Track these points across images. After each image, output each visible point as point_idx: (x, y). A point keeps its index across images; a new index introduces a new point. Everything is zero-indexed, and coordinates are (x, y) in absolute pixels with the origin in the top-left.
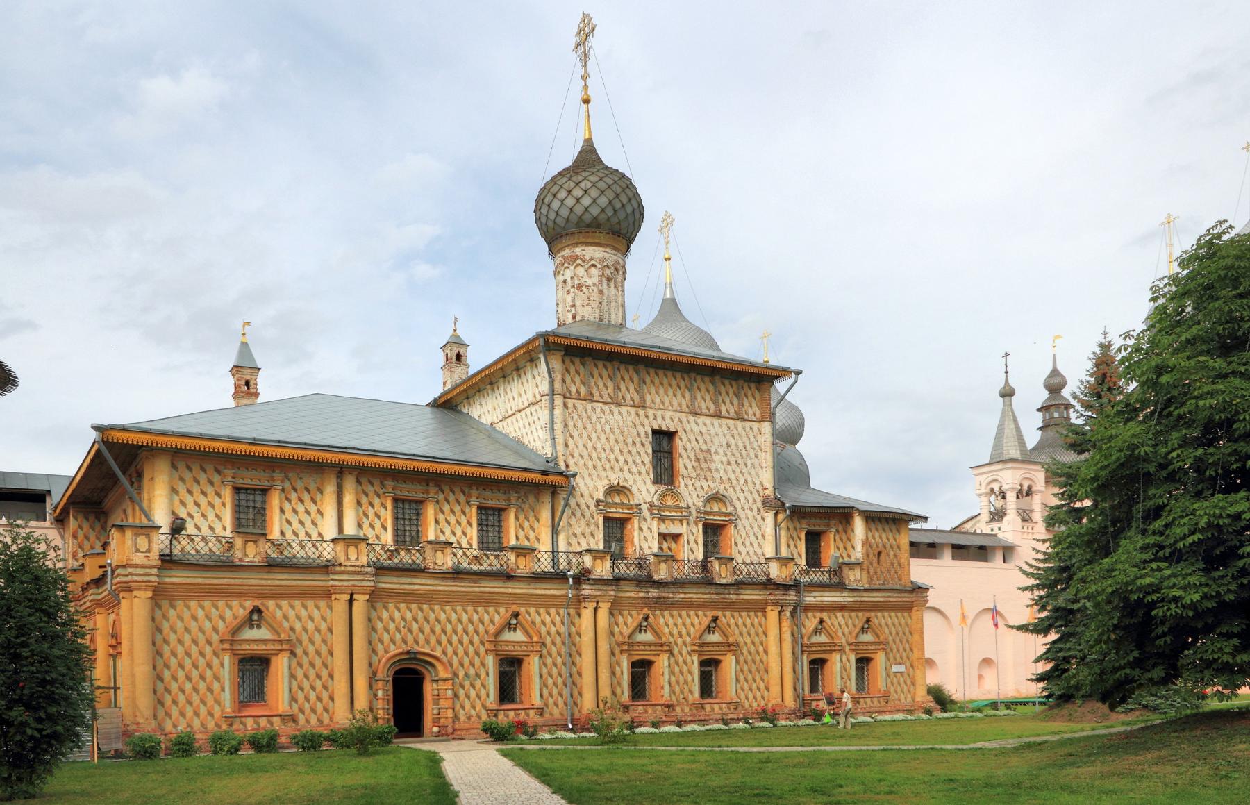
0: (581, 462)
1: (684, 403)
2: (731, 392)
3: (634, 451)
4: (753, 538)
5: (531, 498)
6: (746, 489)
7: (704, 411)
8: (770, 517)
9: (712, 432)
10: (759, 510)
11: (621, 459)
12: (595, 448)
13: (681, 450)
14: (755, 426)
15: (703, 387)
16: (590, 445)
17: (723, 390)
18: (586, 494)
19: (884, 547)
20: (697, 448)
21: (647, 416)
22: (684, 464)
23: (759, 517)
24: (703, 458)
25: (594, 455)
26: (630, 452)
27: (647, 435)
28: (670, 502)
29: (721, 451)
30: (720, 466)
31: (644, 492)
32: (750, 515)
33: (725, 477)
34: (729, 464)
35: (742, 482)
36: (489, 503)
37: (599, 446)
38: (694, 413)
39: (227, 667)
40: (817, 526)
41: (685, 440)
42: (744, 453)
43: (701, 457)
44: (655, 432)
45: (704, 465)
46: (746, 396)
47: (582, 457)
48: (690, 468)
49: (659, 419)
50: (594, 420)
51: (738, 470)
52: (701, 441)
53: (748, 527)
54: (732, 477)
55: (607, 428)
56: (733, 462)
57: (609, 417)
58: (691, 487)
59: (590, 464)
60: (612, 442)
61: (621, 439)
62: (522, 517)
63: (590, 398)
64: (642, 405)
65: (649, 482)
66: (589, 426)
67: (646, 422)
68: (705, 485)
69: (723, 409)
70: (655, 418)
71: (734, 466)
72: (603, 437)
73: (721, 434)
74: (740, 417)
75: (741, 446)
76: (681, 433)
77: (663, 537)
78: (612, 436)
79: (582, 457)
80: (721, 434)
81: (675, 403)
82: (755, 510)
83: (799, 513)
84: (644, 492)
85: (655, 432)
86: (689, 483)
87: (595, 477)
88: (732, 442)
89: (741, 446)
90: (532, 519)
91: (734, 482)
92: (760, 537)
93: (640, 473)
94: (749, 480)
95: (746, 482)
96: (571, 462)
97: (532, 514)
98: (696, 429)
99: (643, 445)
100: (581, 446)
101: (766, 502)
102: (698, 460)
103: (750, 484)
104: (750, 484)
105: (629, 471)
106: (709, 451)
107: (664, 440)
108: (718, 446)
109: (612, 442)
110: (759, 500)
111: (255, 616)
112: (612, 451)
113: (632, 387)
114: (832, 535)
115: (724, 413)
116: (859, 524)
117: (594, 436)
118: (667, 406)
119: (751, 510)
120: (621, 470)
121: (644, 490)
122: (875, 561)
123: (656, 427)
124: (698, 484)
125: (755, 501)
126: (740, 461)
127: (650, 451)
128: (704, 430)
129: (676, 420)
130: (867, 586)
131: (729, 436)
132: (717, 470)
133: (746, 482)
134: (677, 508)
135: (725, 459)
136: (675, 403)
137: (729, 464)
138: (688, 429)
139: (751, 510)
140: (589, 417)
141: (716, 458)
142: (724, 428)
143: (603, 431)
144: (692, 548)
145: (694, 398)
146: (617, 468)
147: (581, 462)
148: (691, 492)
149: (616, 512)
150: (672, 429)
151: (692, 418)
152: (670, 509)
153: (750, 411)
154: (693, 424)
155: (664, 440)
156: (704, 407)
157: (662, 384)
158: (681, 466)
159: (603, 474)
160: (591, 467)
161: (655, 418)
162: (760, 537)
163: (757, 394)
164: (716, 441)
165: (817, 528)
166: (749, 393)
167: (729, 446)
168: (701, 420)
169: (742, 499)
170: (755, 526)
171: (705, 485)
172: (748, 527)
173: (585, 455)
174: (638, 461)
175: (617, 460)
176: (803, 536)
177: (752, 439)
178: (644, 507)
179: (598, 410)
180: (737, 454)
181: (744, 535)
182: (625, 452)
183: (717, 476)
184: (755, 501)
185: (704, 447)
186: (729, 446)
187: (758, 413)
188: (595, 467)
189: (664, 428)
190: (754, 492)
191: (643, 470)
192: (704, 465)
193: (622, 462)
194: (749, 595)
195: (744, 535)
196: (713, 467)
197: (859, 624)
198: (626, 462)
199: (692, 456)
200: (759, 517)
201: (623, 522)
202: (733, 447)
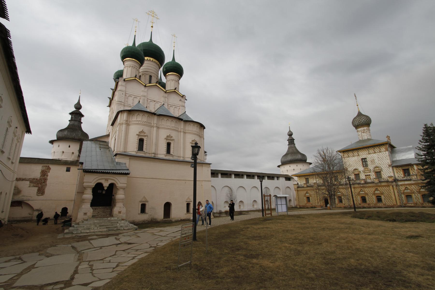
8: (391, 168)
22: (369, 163)
24: (373, 161)
28: (366, 170)
38: (369, 154)
39: (305, 198)
63: (349, 157)
64: (359, 155)
74: (380, 152)
77: (366, 175)
83: (397, 167)
85: (362, 159)
101: (389, 166)
107: (364, 161)
111: (307, 193)
114: (410, 169)
116: (415, 167)
118: (363, 154)
121: (361, 168)
144: (373, 176)
148: (371, 167)
155: (364, 161)
194: (383, 184)
201: (359, 174)
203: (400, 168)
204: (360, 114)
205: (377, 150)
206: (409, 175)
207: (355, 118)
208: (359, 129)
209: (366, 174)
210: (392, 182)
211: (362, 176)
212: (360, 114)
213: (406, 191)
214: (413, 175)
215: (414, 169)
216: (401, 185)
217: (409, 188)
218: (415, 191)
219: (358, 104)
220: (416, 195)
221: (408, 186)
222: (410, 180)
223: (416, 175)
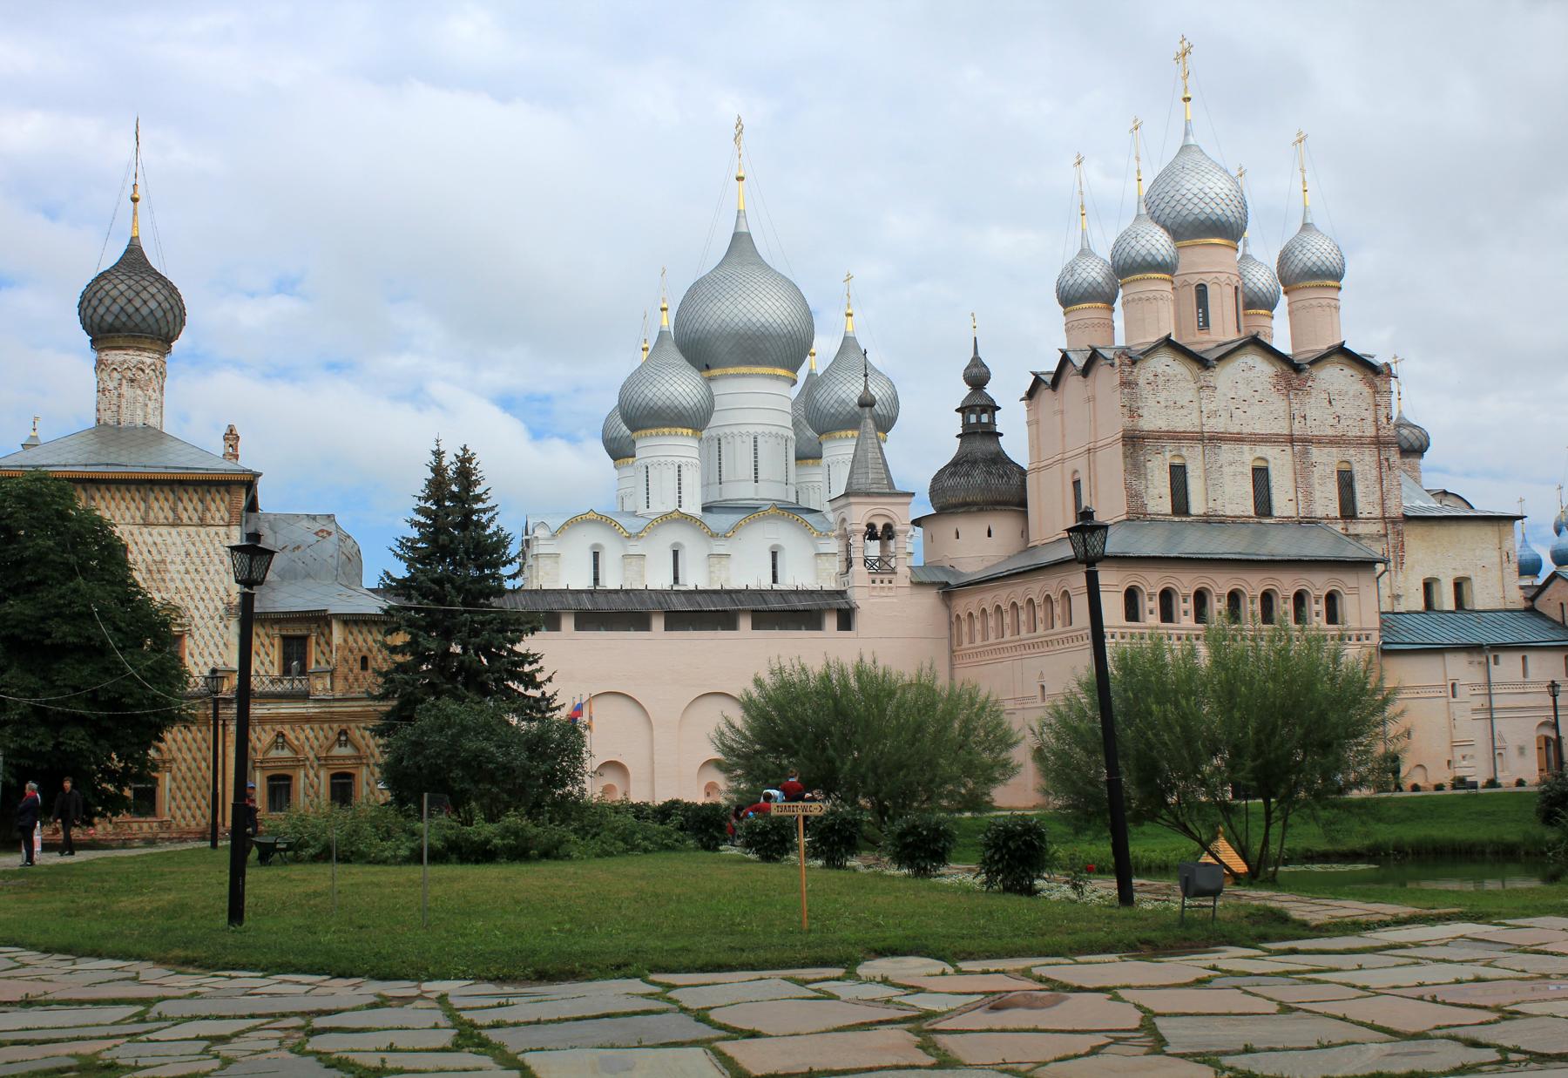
1: (138, 515)
2: (195, 498)
4: (212, 648)
6: (206, 597)
7: (162, 521)
9: (169, 541)
14: (222, 530)
15: (161, 497)
17: (185, 497)
19: (370, 650)
20: (149, 558)
29: (178, 560)
30: (175, 576)
32: (211, 624)
33: (181, 586)
34: (187, 572)
38: (146, 524)
40: (298, 631)
41: (135, 551)
42: (206, 560)
43: (154, 568)
45: (156, 576)
51: (198, 577)
52: (154, 552)
53: (207, 637)
54: (191, 586)
56: (192, 569)
69: (185, 516)
71: (194, 575)
73: (178, 542)
74: (202, 523)
75: (203, 552)
80: (178, 542)
81: (128, 516)
88: (193, 550)
89: (203, 552)
91: (193, 591)
94: (212, 588)
95: (207, 589)
98: (150, 540)
101: (228, 609)
102: (150, 571)
106: (163, 561)
108: (175, 557)
110: (221, 607)
115: (186, 520)
119: (212, 618)
122: (357, 667)
126: (201, 569)
128: (159, 540)
130: (338, 695)
131: (189, 545)
132: (172, 580)
133: (207, 589)
135: (182, 569)
136: (128, 516)
138: (140, 540)
141: (171, 568)
142: (184, 536)
145: (148, 508)
151: (145, 530)
153: (218, 515)
154: (146, 536)
156: (161, 515)
162: (221, 645)
163: (227, 498)
164: (173, 550)
165: (298, 633)
167: (187, 554)
168: (155, 531)
169: (202, 608)
170: (216, 635)
172: (207, 637)
176: (277, 642)
180: (197, 561)
181: (202, 645)
183: (172, 586)
185: (158, 558)
186: (187, 554)
187: (226, 517)
190: (216, 599)
192: (156, 576)
195: (202, 645)
196: (167, 577)
197: (332, 736)
200: (221, 626)
202: (193, 554)
203: (276, 631)
204: (134, 260)
205: (189, 506)
206: (303, 671)
207: (102, 276)
208: (115, 356)
212: (134, 260)
213: (273, 754)
214: (319, 674)
215: (329, 644)
216: (263, 721)
217: (291, 736)
218: (311, 755)
219: (140, 193)
220: (311, 773)
221: (287, 729)
222: (304, 696)
223: (332, 673)
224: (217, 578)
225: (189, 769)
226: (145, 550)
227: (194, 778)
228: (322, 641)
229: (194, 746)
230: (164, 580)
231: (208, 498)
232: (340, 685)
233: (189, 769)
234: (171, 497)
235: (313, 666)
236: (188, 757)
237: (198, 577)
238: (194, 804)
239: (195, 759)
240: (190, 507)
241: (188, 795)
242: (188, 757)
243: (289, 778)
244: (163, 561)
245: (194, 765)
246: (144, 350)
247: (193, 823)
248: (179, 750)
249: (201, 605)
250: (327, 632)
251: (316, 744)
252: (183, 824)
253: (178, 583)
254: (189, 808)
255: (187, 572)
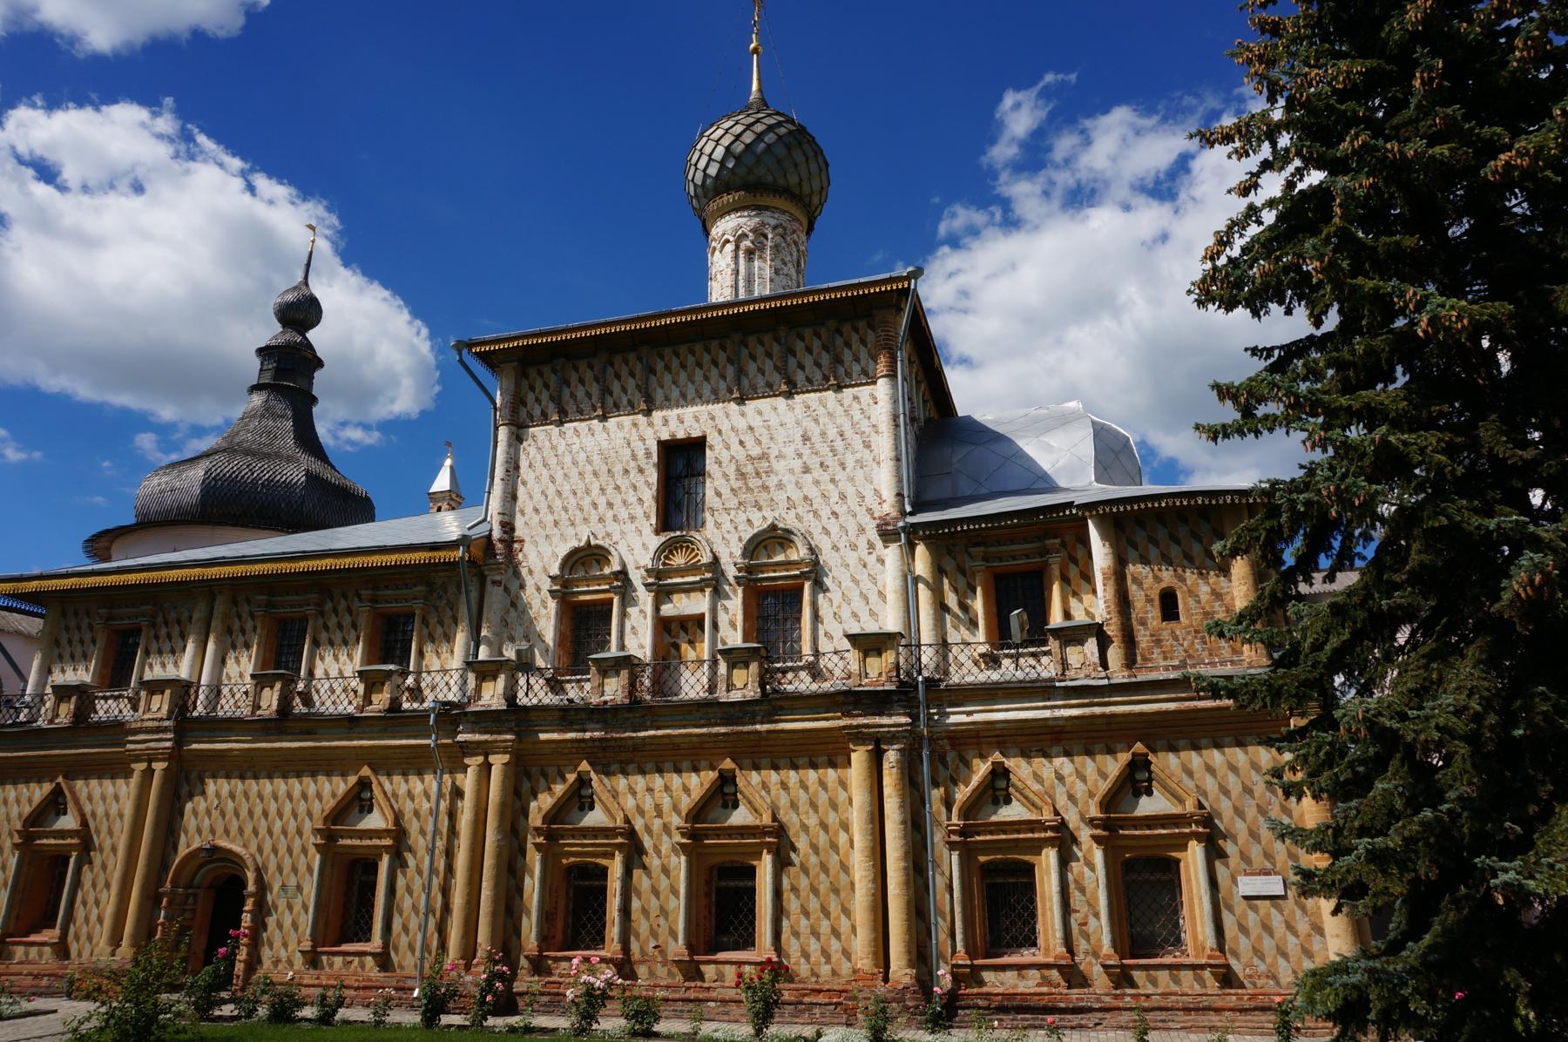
0: (536, 519)
3: (624, 483)
4: (858, 604)
5: (452, 589)
8: (892, 554)
9: (774, 422)
10: (871, 546)
11: (602, 501)
12: (559, 493)
13: (710, 465)
16: (551, 491)
18: (537, 569)
20: (740, 454)
21: (651, 424)
23: (871, 560)
25: (558, 504)
26: (617, 488)
27: (648, 455)
29: (789, 451)
31: (637, 546)
32: (852, 557)
33: (796, 496)
35: (835, 498)
36: (393, 607)
37: (566, 489)
40: (1017, 557)
42: (839, 445)
43: (749, 469)
44: (661, 443)
45: (754, 483)
46: (848, 345)
47: (537, 511)
48: (726, 492)
49: (673, 424)
50: (561, 448)
51: (825, 477)
52: (749, 441)
53: (847, 583)
54: (813, 492)
55: (582, 457)
56: (814, 462)
57: (589, 442)
58: (727, 526)
59: (549, 519)
60: (589, 477)
61: (604, 468)
62: (433, 620)
65: (648, 530)
66: (553, 461)
67: (649, 433)
68: (756, 517)
70: (666, 422)
71: (817, 473)
72: (574, 472)
75: (832, 433)
76: (713, 439)
78: (589, 468)
79: (537, 511)
82: (863, 544)
84: (637, 546)
86: (724, 519)
87: (555, 540)
88: (815, 432)
89: (832, 433)
90: (447, 621)
91: (818, 502)
92: (874, 598)
93: (632, 518)
94: (850, 491)
95: (843, 497)
96: (519, 522)
97: (449, 613)
98: (741, 424)
99: (641, 471)
100: (537, 496)
103: (852, 501)
104: (852, 501)
105: (615, 518)
106: (764, 456)
109: (589, 477)
112: (588, 492)
113: (631, 384)
117: (559, 476)
119: (854, 547)
120: (601, 520)
121: (636, 545)
122: (1153, 614)
123: (665, 436)
124: (742, 517)
125: (862, 530)
126: (830, 461)
127: (653, 476)
128: (756, 422)
129: (704, 417)
130: (1119, 676)
132: (780, 486)
133: (843, 497)
134: (694, 568)
135: (797, 465)
137: (806, 470)
138: (725, 427)
139: (854, 547)
140: (554, 448)
141: (779, 466)
143: (575, 463)
146: (594, 518)
147: (536, 519)
148: (723, 535)
149: (587, 592)
150: (696, 434)
152: (681, 571)
157: (699, 365)
158: (709, 493)
159: (570, 531)
160: (550, 524)
161: (666, 422)
162: (874, 598)
164: (781, 436)
166: (855, 338)
167: (806, 438)
171: (756, 517)
172: (847, 583)
173: (543, 507)
174: (632, 499)
175: (595, 505)
177: (857, 416)
178: (636, 577)
179: (570, 433)
180: (824, 449)
182: (610, 490)
183: (780, 497)
184: (862, 530)
185: (756, 452)
186: (806, 438)
188: (556, 523)
189: (681, 435)
191: (639, 512)
193: (602, 506)
196: (772, 481)
198: (610, 505)
199: (731, 471)
200: (871, 560)
202: (816, 438)
209: (667, 610)
210: (877, 702)
211: (636, 634)
224: (859, 474)
225: (815, 848)
226: (734, 442)
227: (824, 868)
228: (1073, 572)
229: (823, 798)
230: (765, 488)
231: (839, 341)
232: (1115, 654)
233: (815, 848)
234: (776, 348)
235: (1056, 619)
236: (812, 821)
237: (825, 477)
238: (825, 927)
239: (824, 826)
240: (808, 361)
241: (814, 904)
242: (812, 821)
243: (1029, 870)
244: (764, 456)
245: (822, 840)
246: (767, 208)
247: (825, 970)
248: (794, 805)
249: (833, 527)
250: (1080, 554)
251: (1080, 789)
252: (803, 969)
253: (792, 491)
254: (815, 934)
255: (806, 470)
